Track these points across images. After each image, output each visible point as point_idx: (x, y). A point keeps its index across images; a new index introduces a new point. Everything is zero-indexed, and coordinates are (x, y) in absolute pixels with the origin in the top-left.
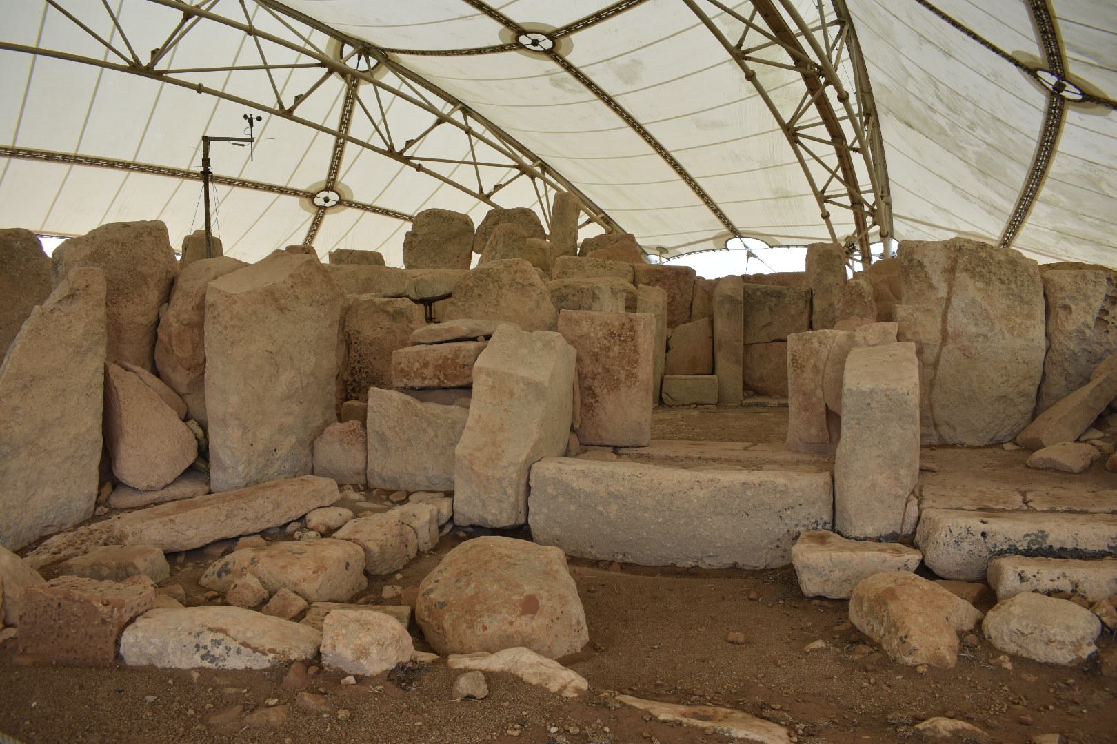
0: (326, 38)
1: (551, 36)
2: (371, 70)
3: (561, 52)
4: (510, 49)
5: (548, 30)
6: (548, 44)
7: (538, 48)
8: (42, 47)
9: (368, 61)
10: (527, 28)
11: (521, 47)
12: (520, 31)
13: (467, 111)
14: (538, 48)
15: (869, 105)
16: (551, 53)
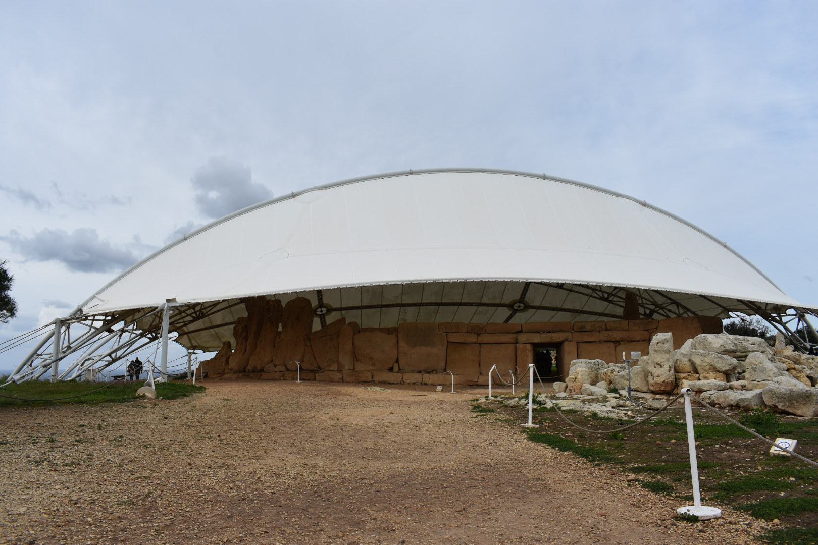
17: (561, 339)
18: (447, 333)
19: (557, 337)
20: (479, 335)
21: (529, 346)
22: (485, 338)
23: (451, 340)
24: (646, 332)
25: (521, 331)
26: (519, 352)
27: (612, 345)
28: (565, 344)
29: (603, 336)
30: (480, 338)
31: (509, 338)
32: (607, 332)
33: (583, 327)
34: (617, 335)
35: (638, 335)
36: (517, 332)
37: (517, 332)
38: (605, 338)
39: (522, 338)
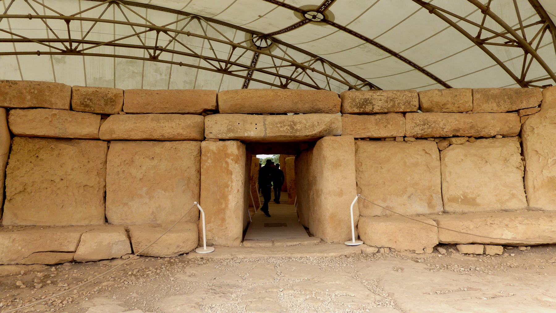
0: (243, 34)
1: (318, 10)
2: (269, 47)
3: (329, 19)
4: (306, 23)
5: (315, 8)
6: (320, 16)
7: (317, 20)
8: (116, 54)
9: (266, 42)
10: (305, 9)
11: (310, 21)
12: (302, 12)
13: (323, 61)
14: (317, 20)
15: (544, 15)
16: (325, 21)
17: (315, 131)
18: (8, 110)
19: (305, 125)
20: (105, 116)
21: (233, 148)
22: (118, 126)
23: (16, 130)
24: (513, 117)
25: (216, 111)
26: (207, 163)
27: (432, 146)
28: (327, 142)
29: (413, 124)
30: (108, 124)
31: (183, 125)
32: (420, 116)
33: (367, 102)
34: (445, 123)
35: (494, 123)
36: (206, 112)
37: (206, 112)
38: (418, 131)
39: (216, 125)
